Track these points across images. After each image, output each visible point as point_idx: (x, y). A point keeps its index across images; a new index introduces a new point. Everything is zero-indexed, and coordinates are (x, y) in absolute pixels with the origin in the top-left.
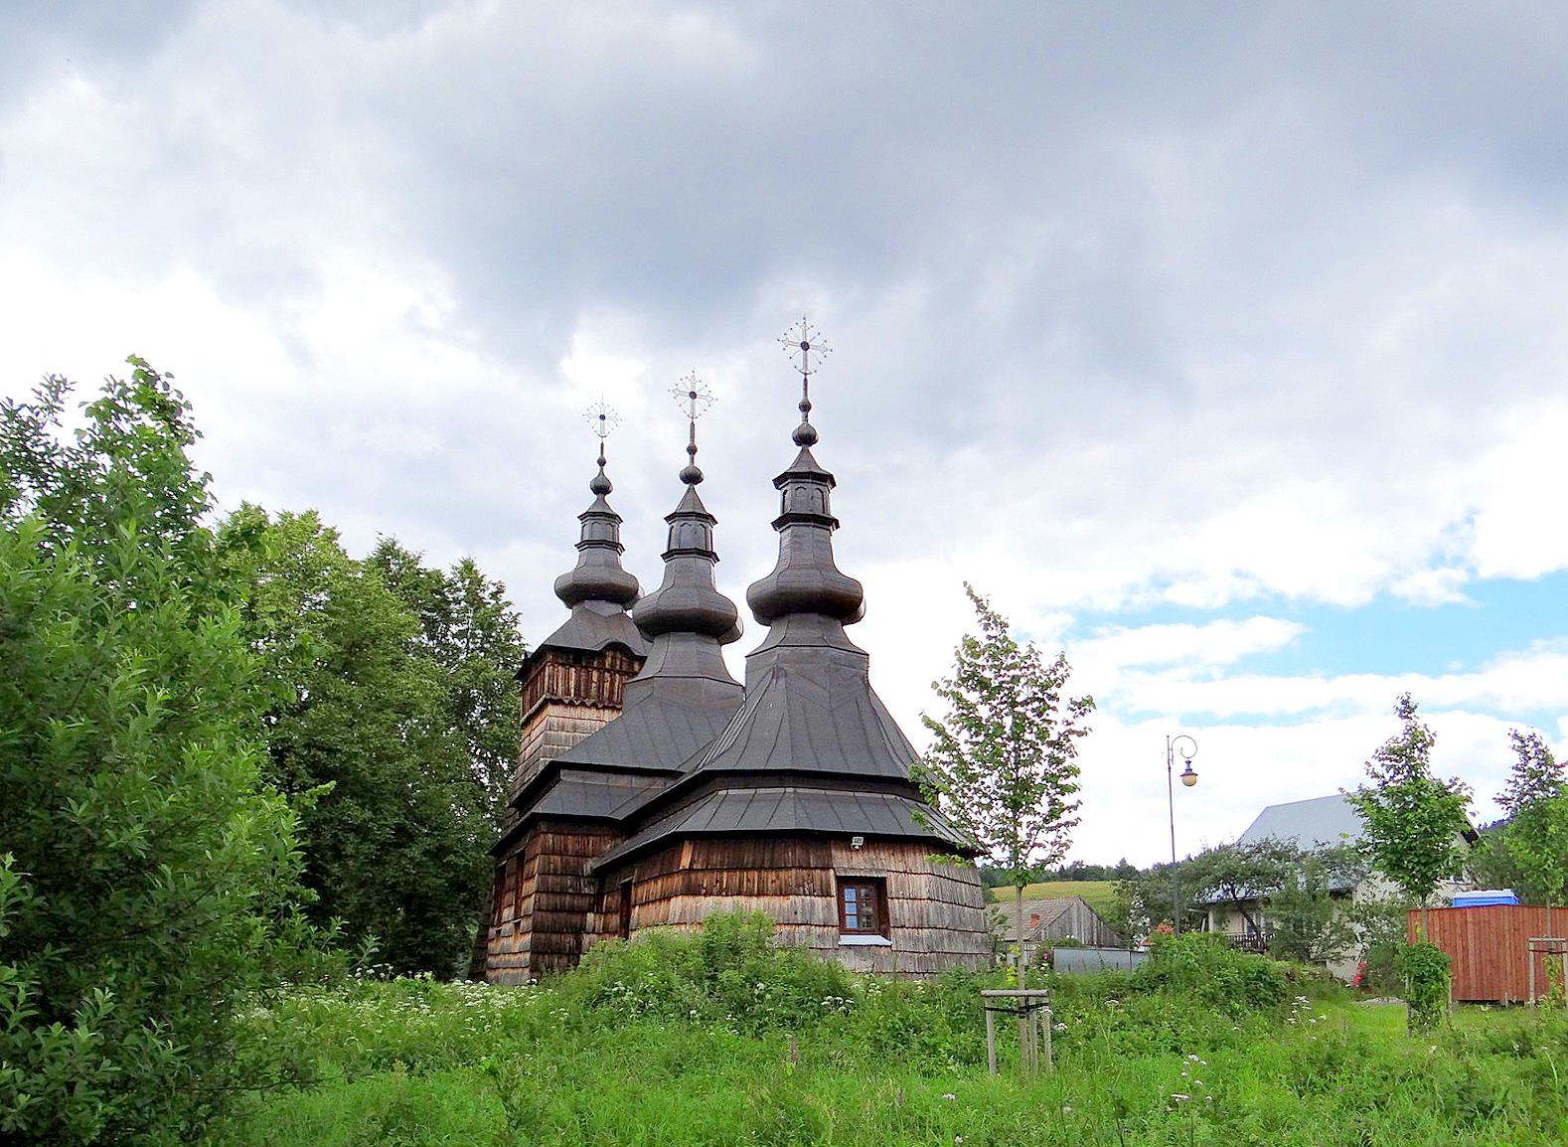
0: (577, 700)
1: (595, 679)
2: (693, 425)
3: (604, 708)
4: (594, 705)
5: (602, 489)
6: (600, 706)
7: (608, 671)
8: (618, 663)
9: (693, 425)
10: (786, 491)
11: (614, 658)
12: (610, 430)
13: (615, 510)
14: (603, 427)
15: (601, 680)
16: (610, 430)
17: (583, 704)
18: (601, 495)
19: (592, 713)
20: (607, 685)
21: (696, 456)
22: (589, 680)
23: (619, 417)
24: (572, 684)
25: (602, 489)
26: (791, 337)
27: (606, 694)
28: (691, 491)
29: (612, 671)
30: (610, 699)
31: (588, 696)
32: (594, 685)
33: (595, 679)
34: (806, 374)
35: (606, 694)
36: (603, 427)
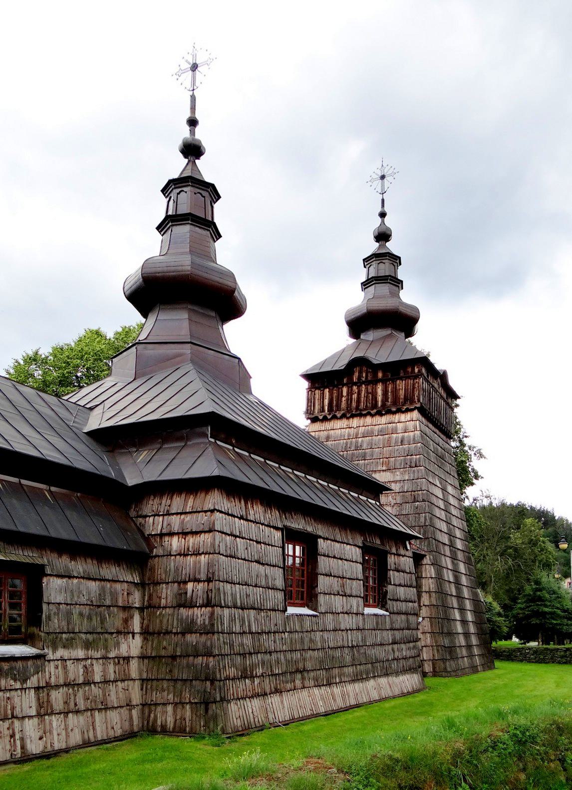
0: (329, 414)
1: (345, 393)
3: (353, 416)
4: (343, 416)
5: (383, 236)
6: (348, 415)
7: (355, 384)
8: (364, 375)
11: (360, 373)
14: (383, 186)
15: (350, 393)
17: (335, 417)
18: (383, 242)
19: (344, 423)
20: (355, 396)
22: (340, 395)
24: (326, 402)
25: (383, 236)
27: (354, 405)
29: (359, 384)
30: (357, 408)
31: (338, 408)
32: (344, 399)
33: (345, 393)
35: (354, 405)
36: (383, 186)
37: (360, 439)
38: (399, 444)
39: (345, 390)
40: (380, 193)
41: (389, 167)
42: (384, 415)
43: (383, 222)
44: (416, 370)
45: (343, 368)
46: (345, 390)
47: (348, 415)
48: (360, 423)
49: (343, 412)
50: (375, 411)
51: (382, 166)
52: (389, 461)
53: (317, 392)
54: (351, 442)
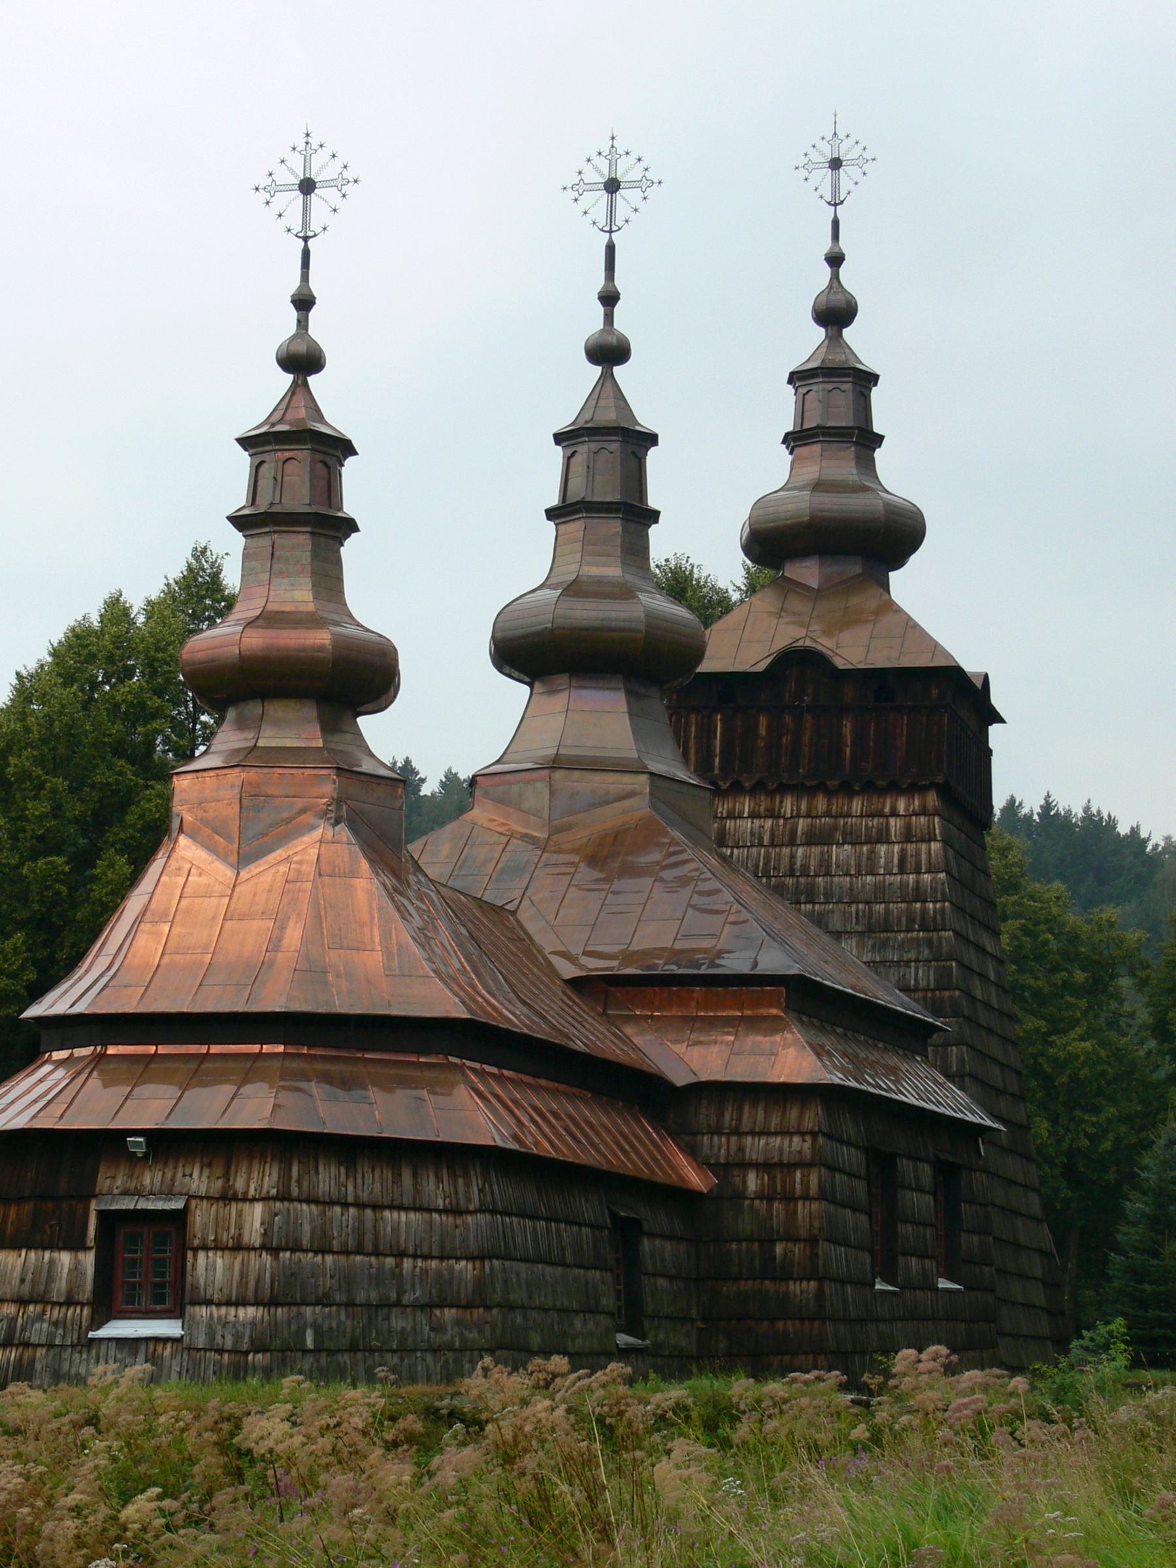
0: (724, 779)
2: (610, 250)
6: (772, 786)
9: (610, 250)
10: (262, 462)
12: (851, 187)
13: (869, 360)
16: (851, 187)
21: (618, 309)
23: (803, 173)
26: (317, 161)
28: (607, 377)
33: (763, 731)
34: (306, 239)
37: (800, 851)
38: (895, 870)
39: (763, 722)
40: (829, 203)
41: (852, 140)
42: (858, 793)
43: (835, 277)
44: (935, 692)
45: (760, 668)
46: (763, 722)
47: (772, 786)
48: (799, 809)
49: (758, 776)
50: (836, 782)
51: (835, 134)
52: (870, 910)
53: (693, 718)
54: (779, 855)
